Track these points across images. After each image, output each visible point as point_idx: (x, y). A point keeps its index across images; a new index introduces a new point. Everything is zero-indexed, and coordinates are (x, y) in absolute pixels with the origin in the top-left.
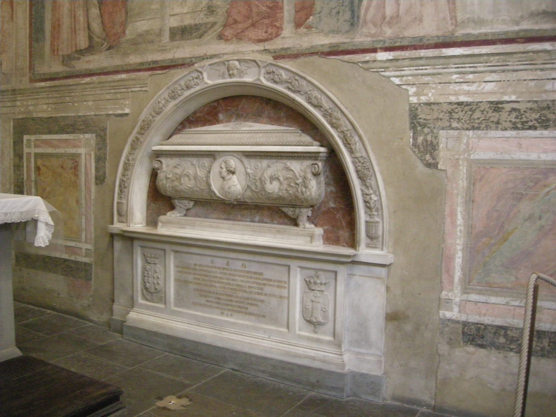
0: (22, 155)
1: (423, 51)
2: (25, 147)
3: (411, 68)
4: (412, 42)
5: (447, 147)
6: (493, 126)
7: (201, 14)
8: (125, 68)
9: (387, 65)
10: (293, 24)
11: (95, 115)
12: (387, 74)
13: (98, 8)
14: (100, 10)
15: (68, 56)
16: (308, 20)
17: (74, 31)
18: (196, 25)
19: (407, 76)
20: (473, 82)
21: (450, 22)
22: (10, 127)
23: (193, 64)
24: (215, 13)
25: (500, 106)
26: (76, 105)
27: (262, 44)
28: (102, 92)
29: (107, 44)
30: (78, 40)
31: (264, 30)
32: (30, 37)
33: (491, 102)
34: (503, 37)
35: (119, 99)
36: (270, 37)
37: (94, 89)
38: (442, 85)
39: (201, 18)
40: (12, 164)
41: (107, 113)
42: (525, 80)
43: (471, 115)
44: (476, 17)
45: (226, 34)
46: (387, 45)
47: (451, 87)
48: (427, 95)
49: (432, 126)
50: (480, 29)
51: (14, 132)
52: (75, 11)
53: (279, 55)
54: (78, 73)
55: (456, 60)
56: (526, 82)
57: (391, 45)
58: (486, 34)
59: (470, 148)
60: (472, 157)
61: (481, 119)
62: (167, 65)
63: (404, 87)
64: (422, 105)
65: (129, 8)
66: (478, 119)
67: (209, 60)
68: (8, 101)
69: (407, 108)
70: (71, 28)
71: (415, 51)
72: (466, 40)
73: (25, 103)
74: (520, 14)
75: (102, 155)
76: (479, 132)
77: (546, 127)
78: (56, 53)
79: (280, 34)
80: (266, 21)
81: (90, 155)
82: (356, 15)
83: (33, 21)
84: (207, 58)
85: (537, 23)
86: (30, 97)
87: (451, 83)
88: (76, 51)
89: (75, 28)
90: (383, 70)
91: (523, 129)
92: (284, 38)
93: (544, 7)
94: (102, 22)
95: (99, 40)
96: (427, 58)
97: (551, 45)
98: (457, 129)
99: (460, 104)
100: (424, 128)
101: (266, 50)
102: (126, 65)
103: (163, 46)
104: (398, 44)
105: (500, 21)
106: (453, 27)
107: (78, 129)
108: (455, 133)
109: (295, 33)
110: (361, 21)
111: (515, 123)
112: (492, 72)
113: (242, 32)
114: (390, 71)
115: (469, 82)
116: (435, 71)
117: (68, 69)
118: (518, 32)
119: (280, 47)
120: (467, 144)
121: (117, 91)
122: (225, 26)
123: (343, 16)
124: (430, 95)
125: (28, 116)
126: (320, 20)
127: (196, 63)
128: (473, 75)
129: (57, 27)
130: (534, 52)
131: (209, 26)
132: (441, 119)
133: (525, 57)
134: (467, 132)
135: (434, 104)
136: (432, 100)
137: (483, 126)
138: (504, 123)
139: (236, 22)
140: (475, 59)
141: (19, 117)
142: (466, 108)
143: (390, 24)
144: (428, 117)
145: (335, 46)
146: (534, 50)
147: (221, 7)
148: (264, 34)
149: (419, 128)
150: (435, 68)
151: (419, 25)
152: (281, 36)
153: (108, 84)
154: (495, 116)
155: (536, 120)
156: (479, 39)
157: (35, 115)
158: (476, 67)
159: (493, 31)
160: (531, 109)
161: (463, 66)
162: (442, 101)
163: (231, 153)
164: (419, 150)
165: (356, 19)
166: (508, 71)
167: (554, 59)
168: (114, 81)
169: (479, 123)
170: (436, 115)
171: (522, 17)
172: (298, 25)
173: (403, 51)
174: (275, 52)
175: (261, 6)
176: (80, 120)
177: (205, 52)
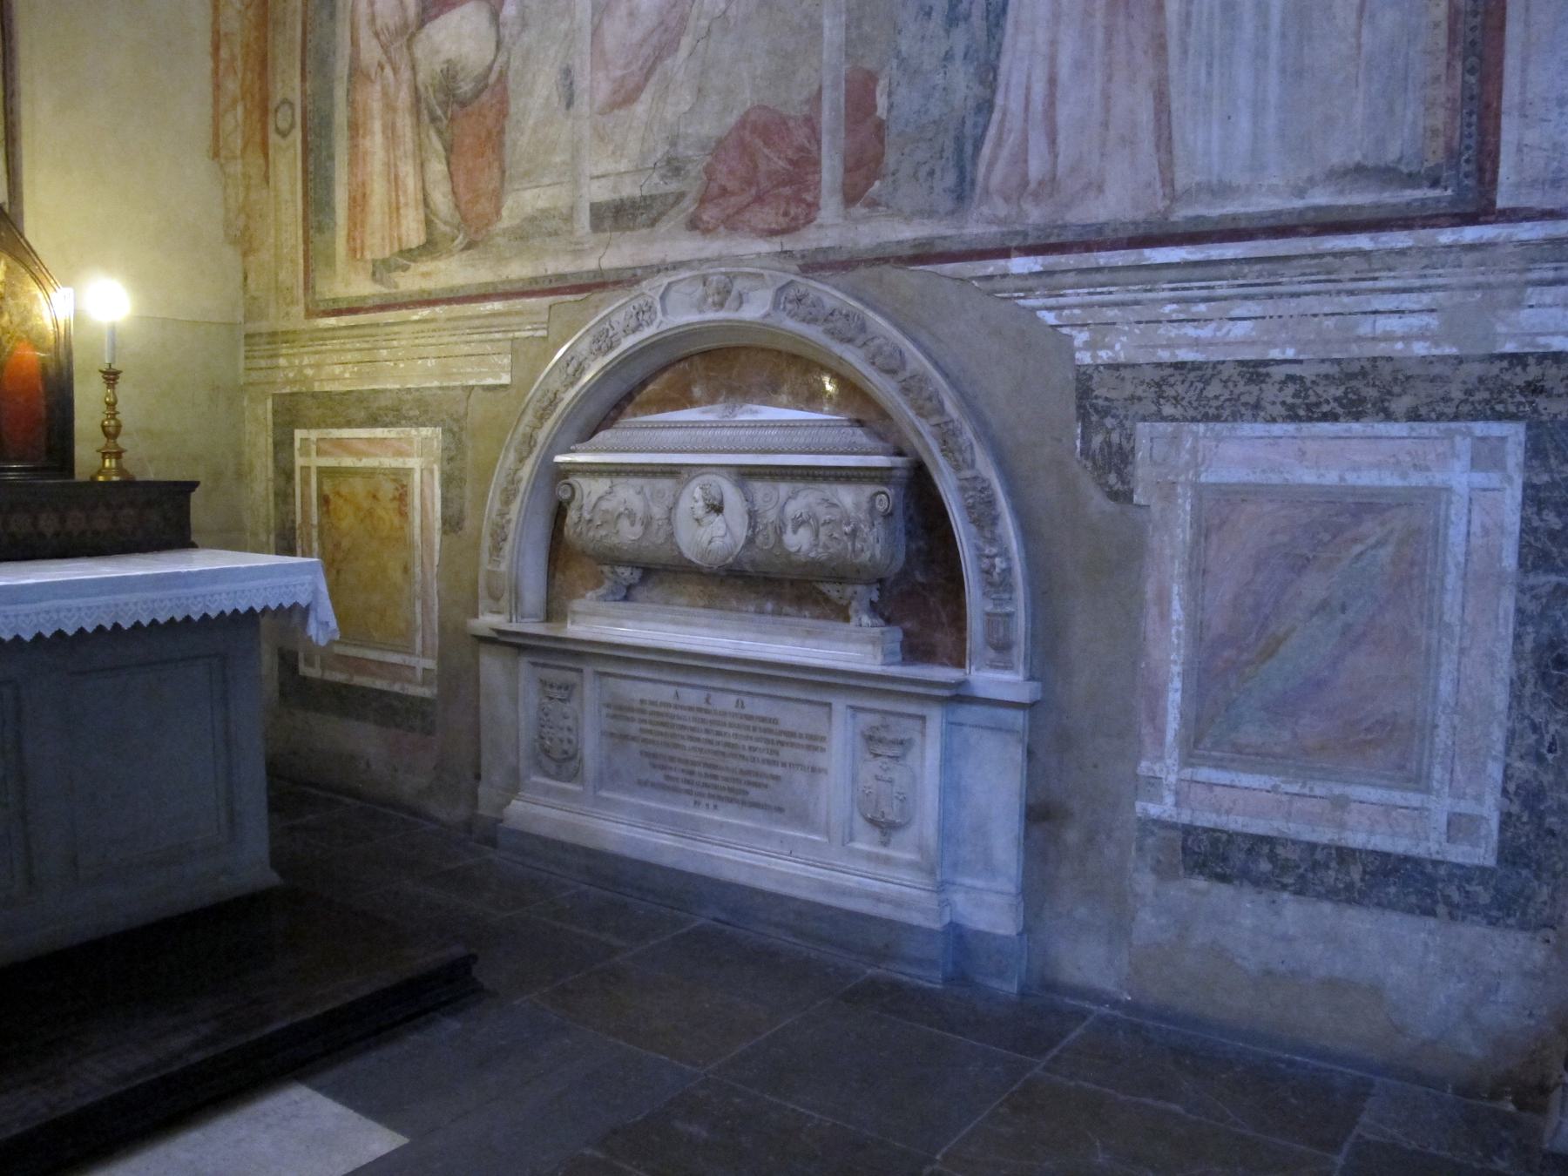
0: (292, 471)
1: (1103, 254)
2: (297, 453)
3: (1079, 291)
4: (1081, 235)
5: (1151, 456)
6: (1248, 413)
7: (655, 175)
8: (501, 288)
9: (1030, 283)
11: (441, 388)
13: (444, 161)
14: (448, 164)
15: (384, 261)
16: (871, 190)
17: (395, 210)
18: (644, 198)
19: (1071, 307)
20: (1206, 320)
21: (1161, 193)
22: (266, 412)
23: (638, 282)
24: (683, 172)
25: (1262, 370)
26: (402, 365)
27: (777, 239)
28: (455, 338)
29: (464, 238)
30: (404, 229)
31: (781, 211)
32: (305, 218)
33: (1242, 363)
34: (1272, 222)
35: (488, 354)
36: (793, 224)
37: (436, 334)
38: (1141, 326)
39: (656, 184)
40: (271, 491)
42: (1315, 315)
43: (1201, 391)
44: (1215, 180)
45: (705, 217)
46: (1030, 241)
47: (1161, 331)
48: (1111, 347)
49: (1121, 412)
51: (274, 424)
53: (814, 265)
54: (406, 299)
55: (1173, 274)
56: (1316, 319)
57: (1039, 242)
58: (1235, 218)
59: (1200, 460)
60: (1203, 479)
61: (1222, 398)
62: (587, 281)
63: (1065, 331)
64: (1101, 368)
65: (507, 161)
66: (1216, 397)
67: (670, 273)
68: (262, 357)
69: (1071, 375)
70: (390, 203)
71: (1086, 254)
72: (1194, 229)
73: (297, 362)
75: (457, 473)
76: (1219, 426)
77: (1357, 417)
78: (358, 256)
79: (815, 219)
80: (787, 191)
81: (431, 472)
82: (968, 179)
83: (311, 185)
84: (667, 269)
85: (1341, 192)
86: (306, 349)
87: (1160, 322)
88: (401, 251)
89: (398, 202)
90: (1022, 294)
91: (1310, 419)
92: (821, 226)
93: (1357, 157)
94: (453, 188)
95: (447, 229)
96: (1113, 269)
97: (1372, 239)
98: (1173, 419)
99: (1179, 366)
100: (1106, 416)
101: (786, 252)
102: (503, 282)
103: (577, 244)
104: (1053, 240)
106: (1168, 202)
107: (405, 418)
108: (1169, 428)
109: (845, 218)
110: (978, 190)
111: (1291, 407)
112: (1246, 297)
113: (737, 213)
114: (1037, 298)
115: (1198, 320)
116: (1129, 297)
117: (385, 290)
118: (1301, 212)
119: (814, 245)
120: (1194, 451)
121: (484, 337)
122: (703, 201)
123: (942, 179)
124: (1118, 347)
125: (304, 389)
126: (895, 189)
127: (645, 279)
128: (1207, 304)
129: (358, 202)
130: (1335, 255)
131: (671, 200)
132: (1140, 399)
133: (1316, 265)
134: (1194, 427)
135: (1125, 366)
136: (1122, 358)
137: (1226, 413)
138: (1269, 407)
140: (1212, 271)
141: (284, 391)
142: (1192, 376)
143: (1036, 196)
144: (1113, 395)
145: (924, 244)
146: (1336, 250)
147: (695, 161)
148: (781, 219)
149: (1094, 418)
150: (1128, 291)
151: (1097, 198)
152: (815, 223)
153: (467, 323)
154: (1251, 393)
155: (1336, 399)
156: (1220, 227)
157: (317, 387)
158: (1213, 288)
159: (1250, 210)
160: (1327, 377)
161: (1186, 285)
162: (1141, 361)
163: (714, 469)
164: (1094, 463)
166: (1281, 295)
167: (1375, 271)
168: (478, 317)
169: (1217, 408)
170: (1129, 389)
171: (1311, 181)
172: (851, 196)
173: (1062, 253)
174: (803, 257)
175: (775, 159)
176: (409, 397)
177: (662, 256)
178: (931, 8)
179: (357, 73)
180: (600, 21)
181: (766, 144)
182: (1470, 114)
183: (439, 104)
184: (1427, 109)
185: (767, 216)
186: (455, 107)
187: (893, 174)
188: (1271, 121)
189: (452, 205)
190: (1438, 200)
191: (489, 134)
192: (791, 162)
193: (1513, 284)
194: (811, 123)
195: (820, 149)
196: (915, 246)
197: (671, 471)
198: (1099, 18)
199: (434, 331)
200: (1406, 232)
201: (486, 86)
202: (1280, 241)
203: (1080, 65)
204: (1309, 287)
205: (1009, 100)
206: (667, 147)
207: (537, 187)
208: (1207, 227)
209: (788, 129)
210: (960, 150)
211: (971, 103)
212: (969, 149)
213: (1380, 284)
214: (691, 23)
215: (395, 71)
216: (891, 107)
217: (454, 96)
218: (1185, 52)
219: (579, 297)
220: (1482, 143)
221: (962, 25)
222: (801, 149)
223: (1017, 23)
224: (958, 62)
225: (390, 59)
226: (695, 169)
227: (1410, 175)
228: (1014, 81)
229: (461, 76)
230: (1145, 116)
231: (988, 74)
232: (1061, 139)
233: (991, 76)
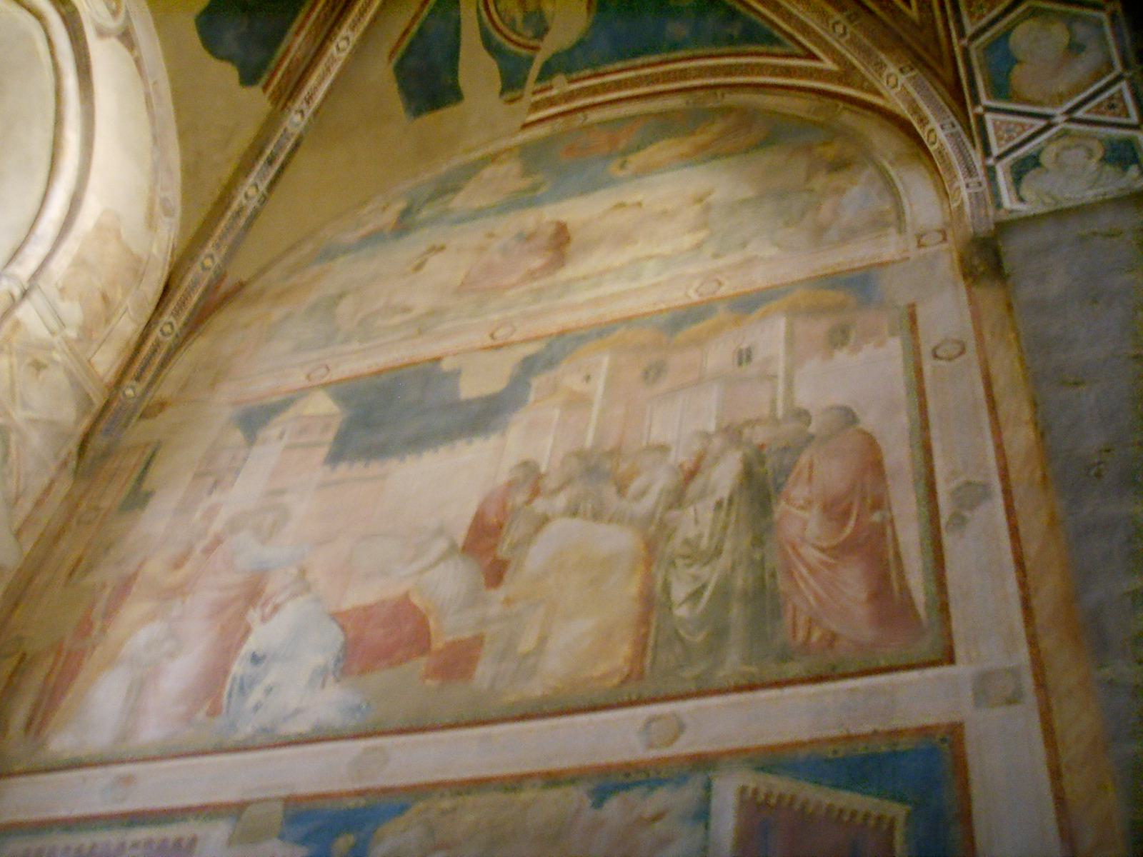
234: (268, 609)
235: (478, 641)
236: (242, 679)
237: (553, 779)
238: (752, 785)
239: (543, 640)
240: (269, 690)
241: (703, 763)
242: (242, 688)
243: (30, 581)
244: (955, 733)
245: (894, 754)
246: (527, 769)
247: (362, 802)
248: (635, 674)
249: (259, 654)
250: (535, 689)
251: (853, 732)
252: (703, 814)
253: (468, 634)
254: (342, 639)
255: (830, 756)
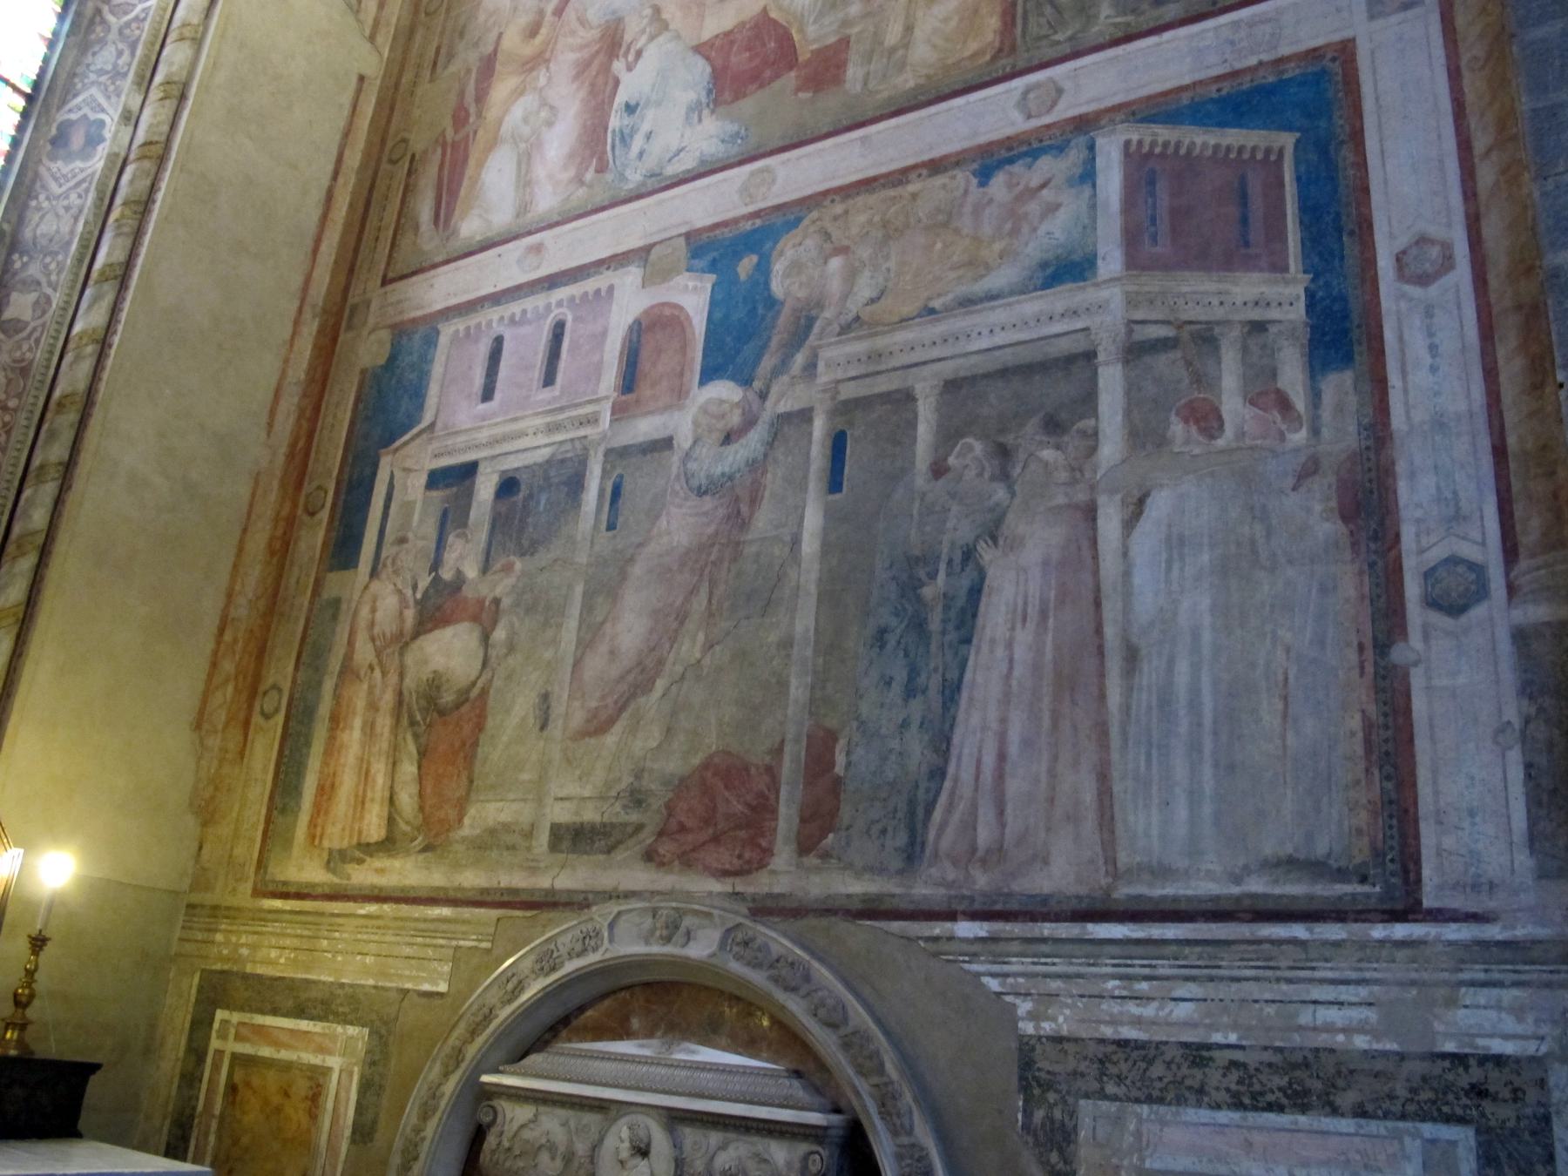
0: (205, 1053)
1: (1047, 925)
2: (214, 1034)
3: (1024, 960)
5: (1094, 1138)
6: (1192, 1098)
8: (452, 894)
9: (976, 948)
10: (794, 846)
11: (375, 987)
12: (975, 967)
14: (419, 768)
17: (361, 803)
18: (604, 825)
19: (1016, 975)
20: (1148, 999)
22: (191, 987)
23: (588, 906)
25: (1205, 1053)
26: (339, 958)
27: (730, 880)
29: (423, 840)
30: (366, 822)
31: (737, 852)
32: (271, 798)
33: (1185, 1045)
34: (1210, 906)
36: (746, 867)
38: (1084, 1000)
39: (616, 813)
40: (178, 1071)
41: (401, 986)
42: (1256, 1001)
43: (1145, 1071)
44: (1155, 863)
45: (661, 851)
46: (977, 906)
47: (1104, 1007)
48: (1054, 1019)
49: (1064, 1087)
50: (1163, 888)
51: (197, 1000)
52: (369, 763)
53: (765, 909)
54: (356, 892)
56: (1257, 1006)
57: (986, 908)
58: (1175, 899)
59: (1144, 1144)
60: (1148, 1164)
61: (1166, 1080)
63: (1009, 999)
64: (1044, 1040)
65: (477, 770)
66: (1160, 1079)
67: (621, 901)
68: (200, 930)
69: (1014, 1045)
70: (356, 796)
73: (234, 939)
74: (1241, 862)
75: (377, 1078)
76: (1162, 1109)
77: (1304, 1109)
78: (317, 842)
79: (768, 864)
80: (742, 834)
81: (351, 1074)
82: (919, 840)
83: (283, 768)
84: (618, 897)
85: (1276, 882)
86: (247, 928)
87: (1103, 997)
88: (359, 845)
89: (364, 796)
90: (967, 958)
91: (1255, 1108)
93: (1289, 849)
95: (408, 829)
98: (1115, 1098)
99: (1122, 1044)
100: (1048, 1090)
101: (737, 894)
104: (998, 907)
105: (1202, 874)
106: (1110, 880)
107: (336, 1014)
108: (1113, 1107)
109: (798, 866)
111: (1236, 1095)
112: (1187, 979)
113: (693, 850)
115: (1141, 998)
117: (336, 880)
118: (1238, 899)
119: (766, 890)
120: (1138, 1134)
121: (428, 941)
122: (661, 834)
124: (1061, 1019)
125: (235, 969)
126: (848, 844)
127: (596, 904)
129: (326, 791)
131: (630, 830)
132: (1083, 1075)
133: (1255, 952)
134: (1137, 1108)
135: (1068, 1039)
136: (1065, 1031)
137: (1170, 1096)
138: (1213, 1093)
139: (682, 829)
140: (1151, 950)
141: (214, 967)
142: (1135, 1054)
144: (1057, 1068)
146: (1274, 937)
148: (735, 861)
149: (1037, 1091)
150: (1071, 964)
151: (1041, 870)
153: (412, 925)
154: (1195, 1077)
155: (1280, 1089)
156: (1162, 907)
157: (249, 969)
158: (1155, 967)
159: (1190, 892)
160: (1270, 1065)
161: (1129, 962)
162: (1084, 1035)
163: (643, 1109)
164: (1036, 1139)
165: (918, 848)
166: (1222, 979)
167: (1312, 961)
168: (425, 920)
169: (1161, 1090)
170: (1071, 1064)
171: (1246, 867)
172: (805, 846)
176: (340, 992)
178: (891, 678)
179: (348, 671)
180: (583, 654)
181: (726, 787)
182: (1391, 816)
183: (419, 710)
184: (1350, 810)
185: (724, 857)
186: (435, 714)
187: (847, 829)
188: (1207, 809)
189: (416, 806)
190: (1368, 896)
191: (464, 744)
192: (748, 805)
193: (1446, 983)
194: (771, 772)
195: (777, 798)
196: (864, 901)
197: (600, 1106)
198: (1046, 703)
199: (379, 928)
200: (1339, 925)
201: (467, 700)
202: (1220, 925)
203: (1027, 743)
204: (1248, 973)
205: (962, 768)
206: (631, 779)
207: (501, 800)
208: (1148, 907)
209: (749, 775)
210: (912, 813)
211: (924, 769)
212: (920, 812)
213: (1318, 974)
214: (668, 667)
215: (384, 674)
216: (849, 764)
217: (436, 704)
218: (1125, 740)
219: (529, 913)
220: (1404, 845)
221: (920, 698)
222: (761, 795)
223: (971, 699)
224: (914, 728)
225: (380, 663)
226: (657, 803)
227: (1339, 870)
228: (966, 751)
229: (444, 688)
230: (1089, 797)
231: (942, 743)
232: (1009, 810)
233: (944, 747)
234: (631, 58)
235: (845, 42)
236: (621, 132)
237: (935, 167)
238: (1135, 137)
239: (909, 29)
240: (649, 136)
241: (1084, 124)
242: (623, 139)
243: (397, 85)
244: (1345, 51)
245: (1282, 84)
246: (910, 162)
247: (758, 222)
248: (1006, 46)
249: (633, 103)
250: (907, 81)
251: (1238, 66)
252: (1088, 175)
253: (832, 39)
254: (709, 69)
255: (1215, 95)
